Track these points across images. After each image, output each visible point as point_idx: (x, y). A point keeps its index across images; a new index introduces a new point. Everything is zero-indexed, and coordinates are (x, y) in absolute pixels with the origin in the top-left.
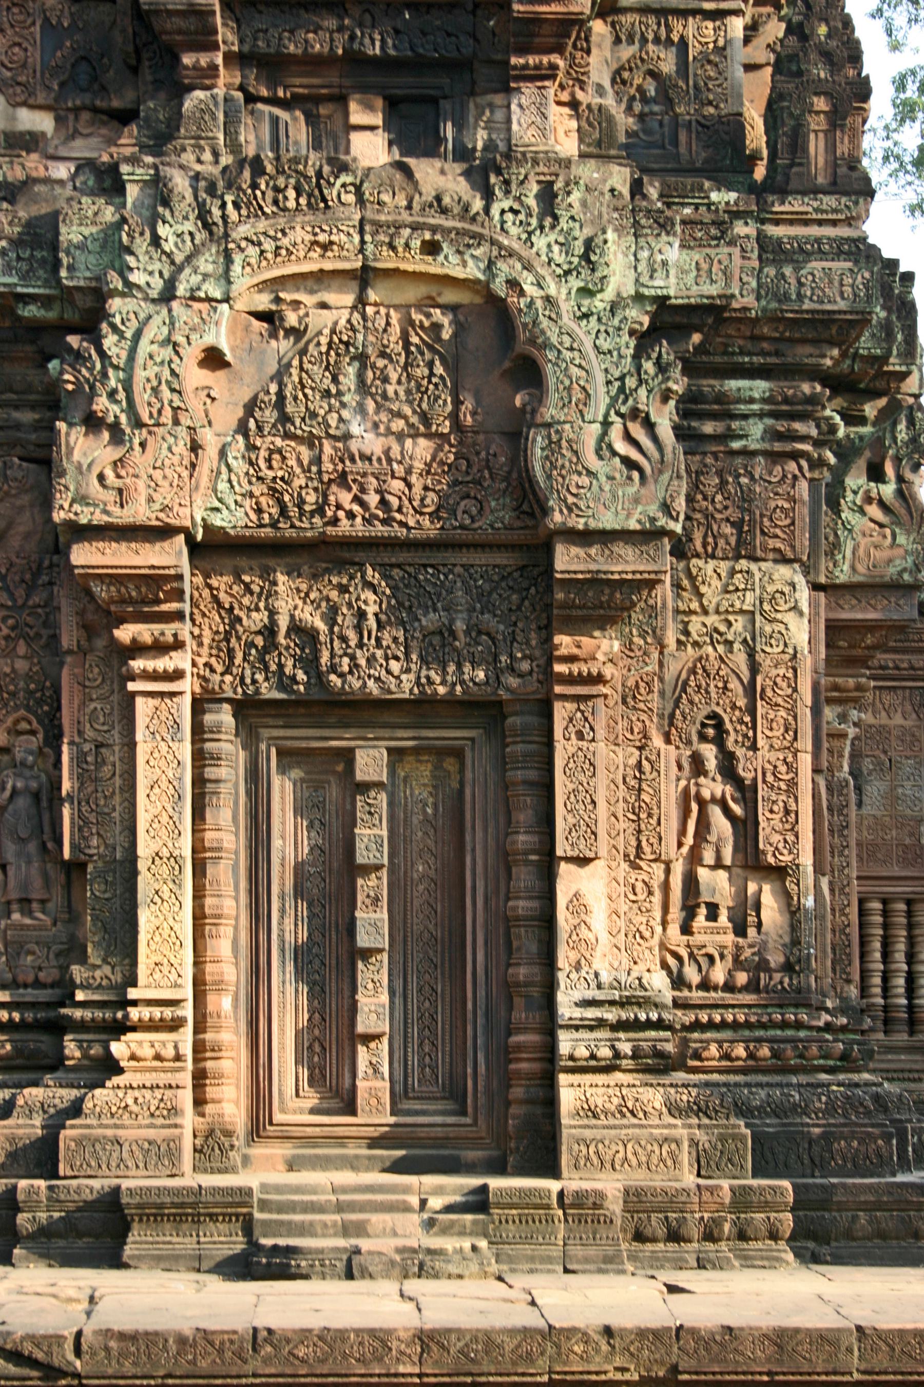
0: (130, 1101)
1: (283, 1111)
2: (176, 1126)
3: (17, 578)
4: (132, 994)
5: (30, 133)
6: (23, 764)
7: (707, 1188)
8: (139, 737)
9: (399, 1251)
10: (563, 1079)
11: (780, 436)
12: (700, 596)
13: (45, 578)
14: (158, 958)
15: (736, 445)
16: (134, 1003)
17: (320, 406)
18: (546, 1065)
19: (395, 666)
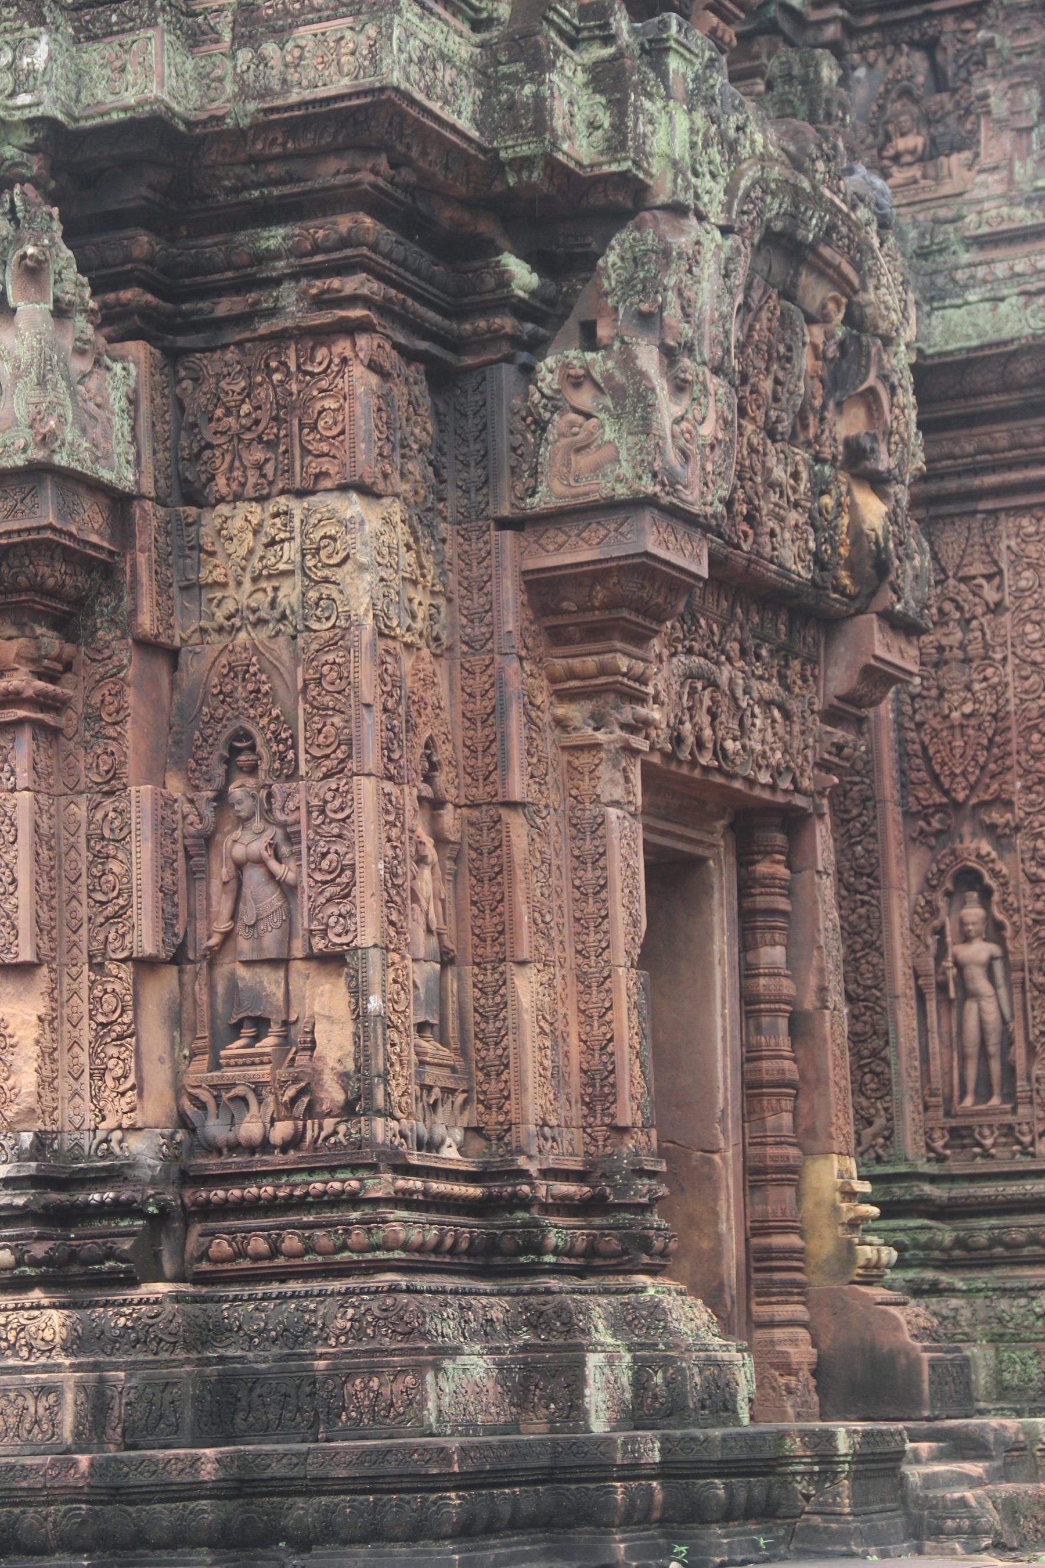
11: (321, 302)
15: (263, 328)
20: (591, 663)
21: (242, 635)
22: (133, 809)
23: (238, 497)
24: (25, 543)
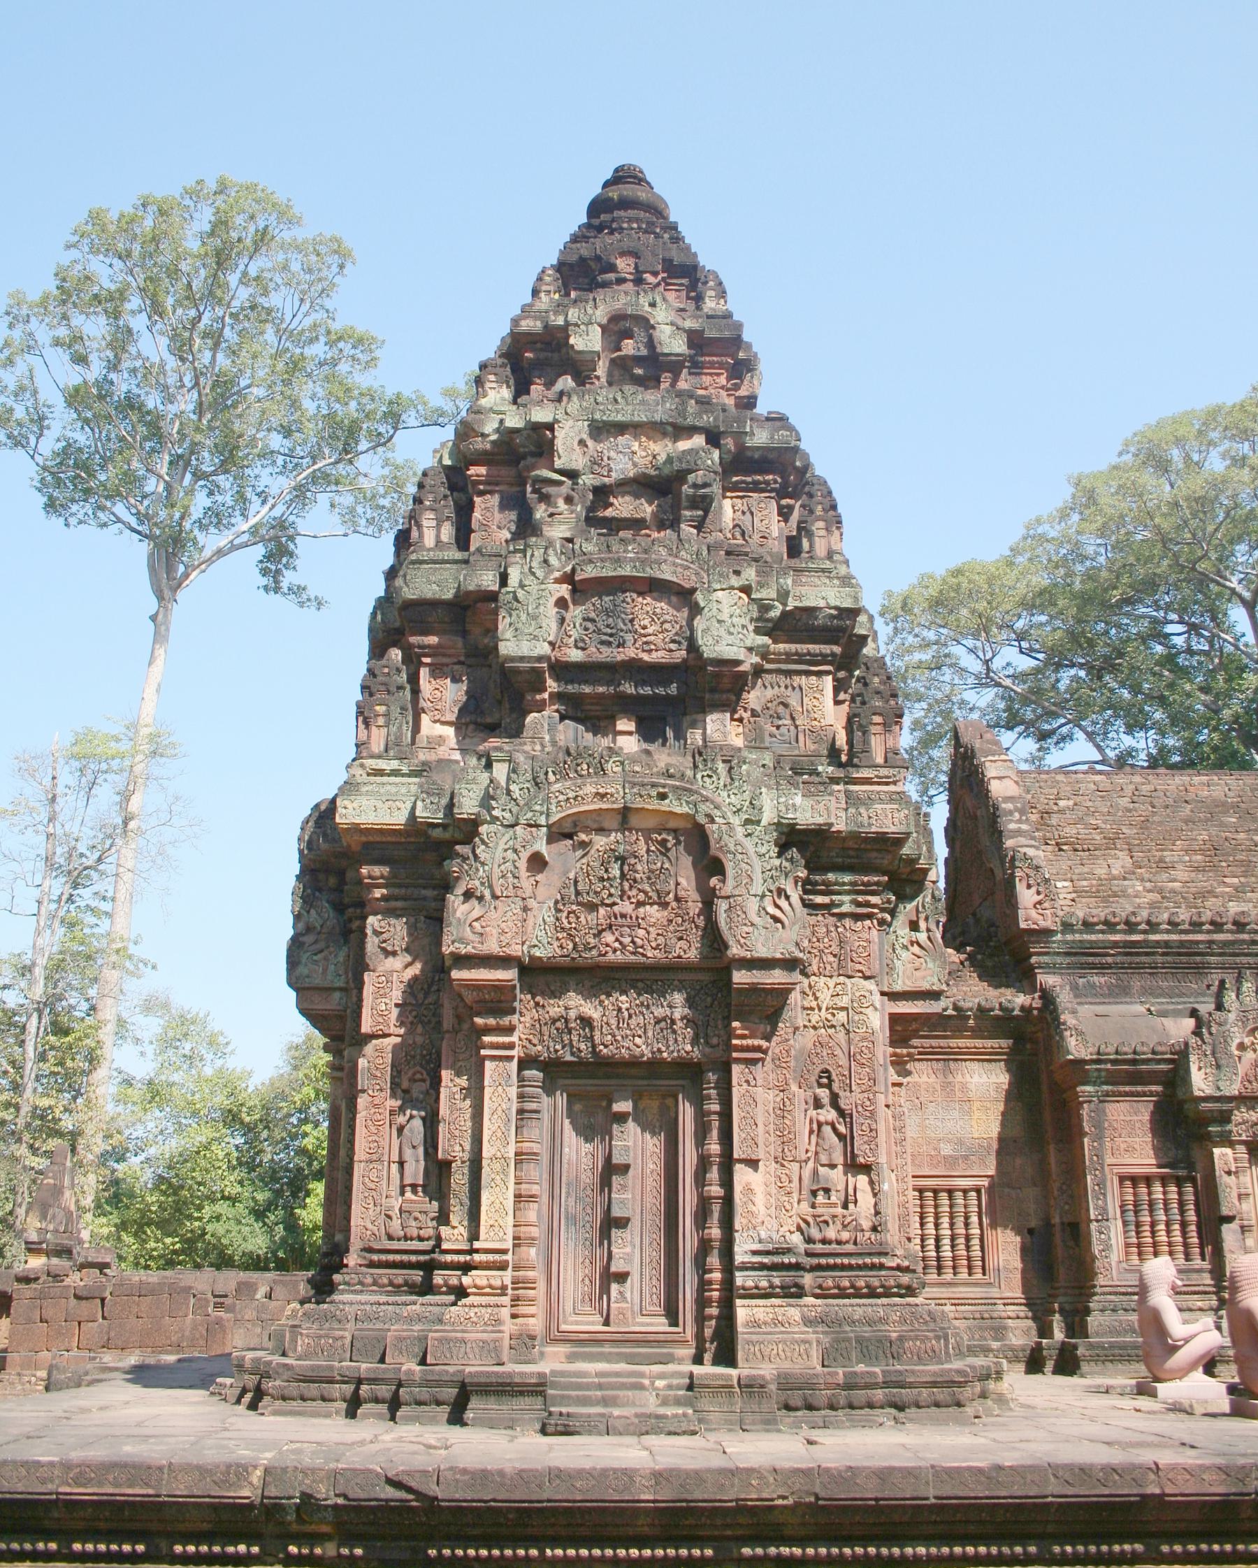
0: (472, 1315)
1: (565, 1323)
2: (500, 1331)
4: (477, 1245)
6: (417, 1099)
7: (829, 1373)
8: (486, 1083)
9: (637, 1415)
10: (738, 1302)
11: (859, 904)
12: (816, 999)
13: (435, 988)
14: (492, 1222)
16: (477, 1251)
17: (598, 887)
18: (728, 1293)
19: (637, 1040)
20: (905, 1051)
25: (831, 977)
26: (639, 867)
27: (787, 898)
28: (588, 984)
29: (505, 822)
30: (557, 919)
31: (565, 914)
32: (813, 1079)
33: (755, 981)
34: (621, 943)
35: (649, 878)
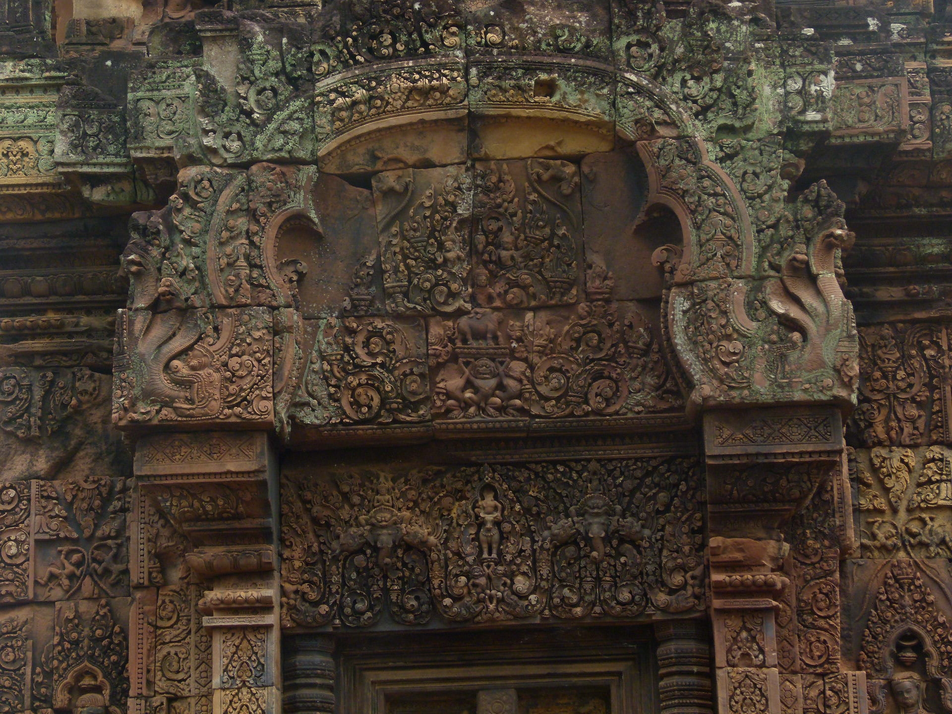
3: (85, 505)
5: (114, 20)
12: (887, 490)
13: (117, 504)
21: (902, 555)
22: (851, 690)
23: (892, 443)
24: (809, 463)
25: (914, 446)
26: (507, 237)
27: (812, 280)
28: (415, 475)
29: (230, 158)
30: (347, 349)
31: (361, 338)
32: (886, 652)
33: (752, 449)
34: (476, 390)
35: (527, 257)
